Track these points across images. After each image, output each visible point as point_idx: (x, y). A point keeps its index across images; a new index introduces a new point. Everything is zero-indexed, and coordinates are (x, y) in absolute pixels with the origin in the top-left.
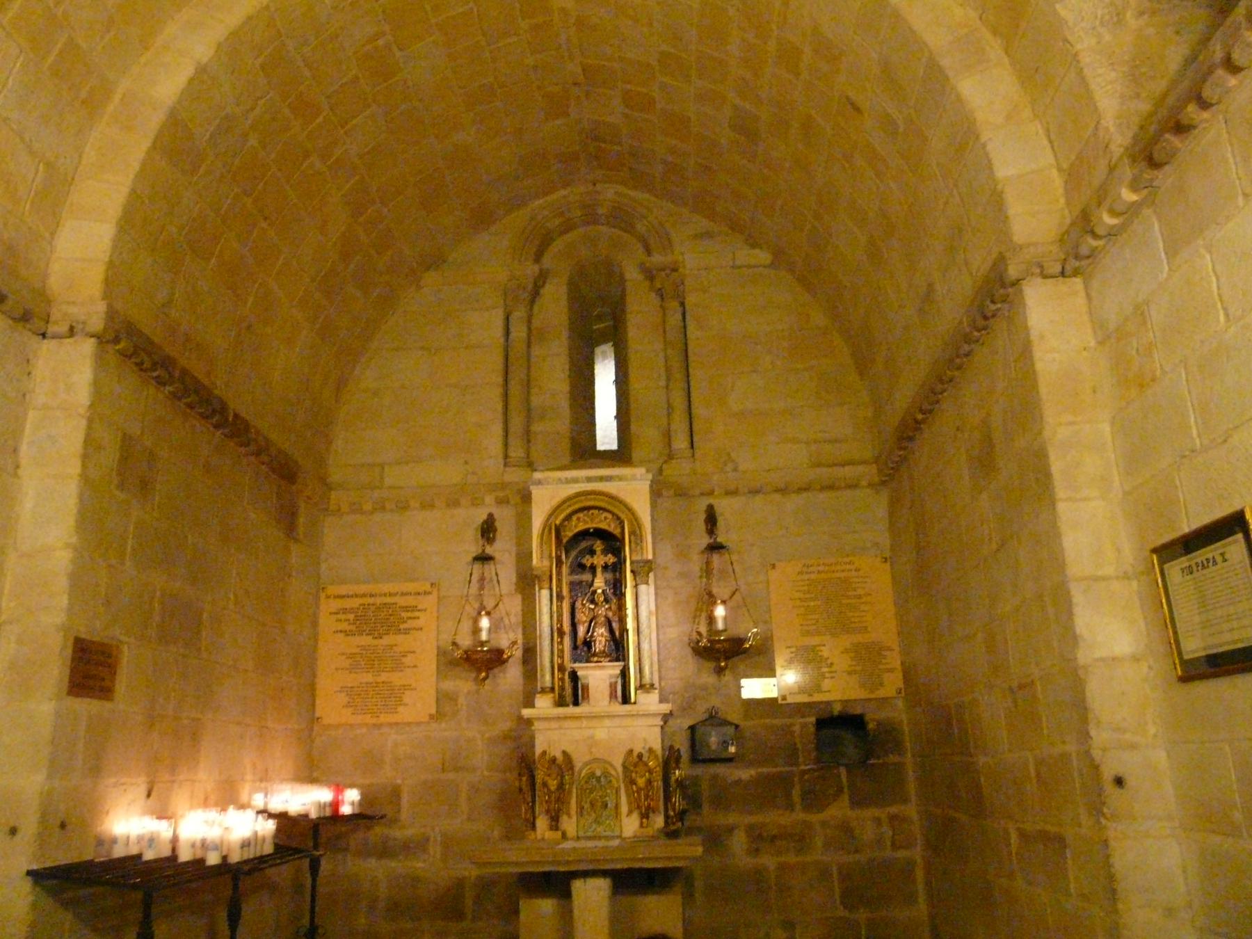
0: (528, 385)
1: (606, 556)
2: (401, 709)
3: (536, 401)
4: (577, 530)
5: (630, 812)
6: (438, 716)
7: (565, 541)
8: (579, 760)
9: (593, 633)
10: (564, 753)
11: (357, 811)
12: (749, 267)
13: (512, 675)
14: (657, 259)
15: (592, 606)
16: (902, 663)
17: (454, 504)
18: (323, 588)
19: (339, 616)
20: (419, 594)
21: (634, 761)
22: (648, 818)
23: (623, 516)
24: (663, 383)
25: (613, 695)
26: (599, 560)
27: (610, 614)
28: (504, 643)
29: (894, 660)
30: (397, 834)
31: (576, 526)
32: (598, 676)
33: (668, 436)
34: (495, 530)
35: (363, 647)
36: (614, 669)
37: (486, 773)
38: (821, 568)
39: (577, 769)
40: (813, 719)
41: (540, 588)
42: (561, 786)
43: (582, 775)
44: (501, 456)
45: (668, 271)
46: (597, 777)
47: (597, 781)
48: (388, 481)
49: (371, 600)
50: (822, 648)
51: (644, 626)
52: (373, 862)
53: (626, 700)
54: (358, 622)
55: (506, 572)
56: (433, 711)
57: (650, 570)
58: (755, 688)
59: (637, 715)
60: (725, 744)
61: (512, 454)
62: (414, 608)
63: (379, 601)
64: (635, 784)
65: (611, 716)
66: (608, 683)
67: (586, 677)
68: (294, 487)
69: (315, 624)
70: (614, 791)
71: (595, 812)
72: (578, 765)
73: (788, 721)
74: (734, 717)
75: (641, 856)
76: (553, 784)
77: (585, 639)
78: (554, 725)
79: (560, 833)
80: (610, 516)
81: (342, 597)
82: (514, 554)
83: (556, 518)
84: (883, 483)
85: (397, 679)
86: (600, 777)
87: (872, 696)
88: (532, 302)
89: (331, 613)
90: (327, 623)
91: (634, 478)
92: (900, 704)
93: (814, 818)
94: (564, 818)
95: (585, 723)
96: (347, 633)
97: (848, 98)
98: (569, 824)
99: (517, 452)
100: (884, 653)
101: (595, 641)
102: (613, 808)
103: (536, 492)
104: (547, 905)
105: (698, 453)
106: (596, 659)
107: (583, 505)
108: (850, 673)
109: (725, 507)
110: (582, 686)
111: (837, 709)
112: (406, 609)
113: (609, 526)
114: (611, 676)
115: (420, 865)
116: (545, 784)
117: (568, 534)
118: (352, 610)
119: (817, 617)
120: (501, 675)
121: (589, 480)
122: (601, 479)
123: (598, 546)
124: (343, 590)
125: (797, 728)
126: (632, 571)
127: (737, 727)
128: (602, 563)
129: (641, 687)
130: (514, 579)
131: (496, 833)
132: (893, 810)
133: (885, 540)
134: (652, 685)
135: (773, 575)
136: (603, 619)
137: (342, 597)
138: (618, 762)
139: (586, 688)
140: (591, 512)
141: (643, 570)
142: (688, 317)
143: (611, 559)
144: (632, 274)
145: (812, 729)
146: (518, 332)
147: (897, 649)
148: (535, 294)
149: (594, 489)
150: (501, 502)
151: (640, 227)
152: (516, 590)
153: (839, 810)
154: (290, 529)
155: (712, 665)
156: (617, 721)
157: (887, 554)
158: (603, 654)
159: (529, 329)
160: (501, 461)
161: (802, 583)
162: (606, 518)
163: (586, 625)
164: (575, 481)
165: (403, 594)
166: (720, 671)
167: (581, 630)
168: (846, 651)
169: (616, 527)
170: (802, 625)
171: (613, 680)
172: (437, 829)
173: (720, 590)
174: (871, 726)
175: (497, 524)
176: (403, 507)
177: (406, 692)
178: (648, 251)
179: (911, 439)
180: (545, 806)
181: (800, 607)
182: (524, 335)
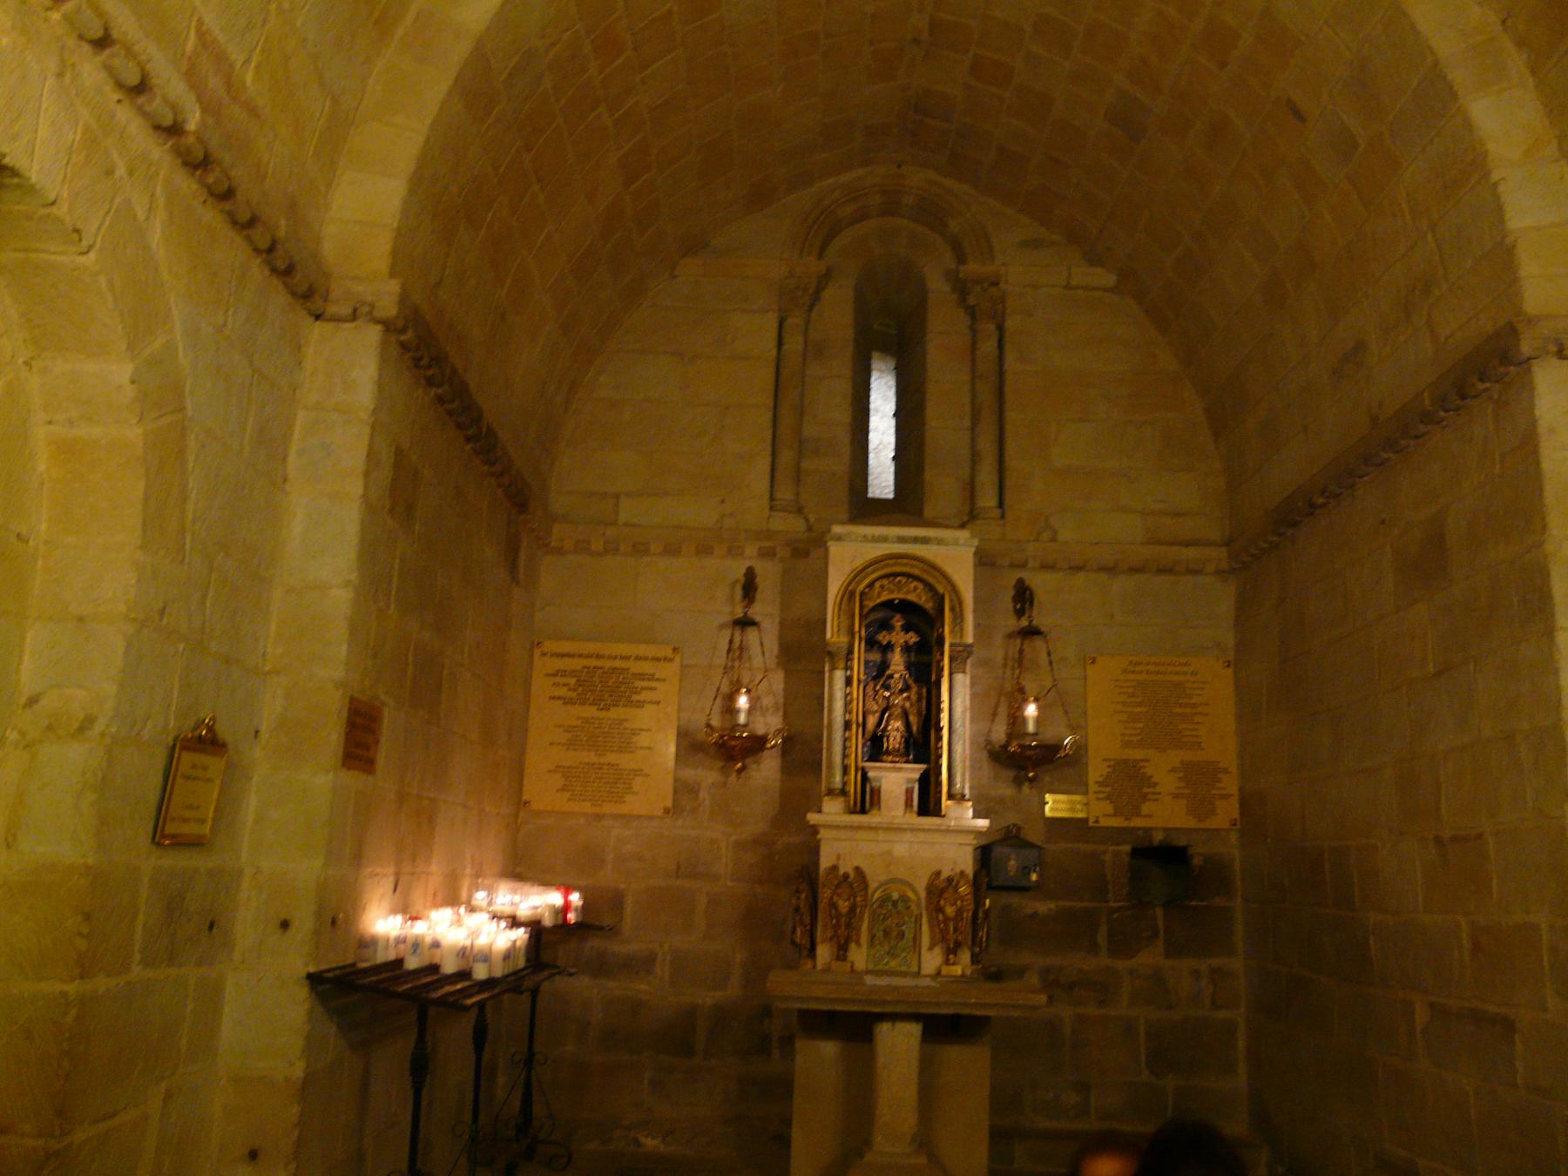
1: (907, 632)
2: (628, 798)
3: (809, 431)
4: (879, 601)
5: (930, 949)
6: (674, 811)
7: (866, 611)
9: (887, 726)
10: (858, 869)
11: (580, 919)
12: (1087, 288)
13: (767, 769)
14: (973, 268)
15: (887, 694)
16: (1241, 789)
17: (704, 550)
18: (538, 644)
19: (558, 679)
20: (658, 660)
21: (939, 889)
22: (955, 954)
23: (941, 590)
24: (967, 423)
25: (908, 803)
26: (899, 637)
27: (908, 704)
28: (760, 730)
29: (1231, 785)
30: (618, 948)
31: (879, 595)
33: (971, 490)
34: (756, 589)
35: (586, 721)
36: (914, 771)
37: (729, 884)
38: (1151, 668)
39: (870, 891)
40: (1127, 848)
41: (833, 669)
42: (853, 909)
43: (874, 900)
44: (767, 496)
45: (986, 285)
46: (893, 902)
47: (893, 907)
48: (622, 518)
49: (594, 663)
50: (1146, 764)
51: (959, 724)
52: (584, 981)
54: (581, 689)
55: (763, 644)
56: (669, 803)
57: (970, 654)
58: (1054, 805)
59: (948, 831)
60: (1026, 871)
61: (778, 495)
62: (651, 677)
63: (608, 664)
64: (943, 913)
65: (914, 830)
66: (904, 787)
67: (879, 780)
68: (522, 517)
69: (527, 683)
70: (913, 919)
71: (889, 943)
72: (873, 885)
73: (1101, 848)
74: (1034, 835)
75: (973, 1001)
76: (844, 906)
77: (875, 733)
78: (843, 834)
79: (849, 965)
80: (921, 586)
81: (562, 656)
82: (777, 620)
83: (859, 583)
84: (1233, 571)
85: (626, 761)
86: (897, 901)
87: (1202, 825)
88: (810, 309)
89: (547, 675)
90: (541, 686)
91: (956, 543)
92: (1233, 837)
93: (1121, 965)
94: (853, 946)
95: (882, 836)
96: (568, 702)
97: (1289, 101)
98: (859, 956)
99: (785, 494)
100: (1220, 775)
101: (888, 737)
102: (911, 939)
103: (834, 548)
104: (829, 1049)
105: (1009, 516)
106: (890, 758)
107: (894, 568)
108: (1176, 796)
109: (1040, 582)
110: (872, 790)
111: (1158, 837)
112: (641, 676)
113: (920, 598)
114: (909, 781)
115: (643, 987)
116: (834, 906)
118: (573, 673)
119: (1141, 725)
120: (754, 766)
121: (902, 540)
122: (916, 540)
123: (898, 622)
124: (565, 647)
125: (1108, 857)
126: (951, 659)
127: (1040, 848)
128: (902, 641)
129: (950, 796)
130: (776, 651)
131: (738, 956)
132: (1216, 962)
133: (1230, 640)
134: (964, 796)
135: (1091, 670)
136: (899, 710)
137: (562, 656)
138: (921, 885)
139: (876, 793)
140: (898, 578)
141: (961, 655)
142: (1008, 347)
143: (913, 638)
144: (937, 286)
145: (1126, 859)
146: (794, 344)
147: (1234, 769)
148: (816, 298)
149: (902, 551)
151: (954, 226)
152: (778, 664)
153: (1150, 958)
154: (513, 568)
155: (1011, 774)
156: (922, 837)
157: (1231, 657)
159: (806, 342)
160: (765, 502)
161: (1128, 684)
162: (915, 588)
163: (877, 715)
164: (884, 539)
165: (638, 658)
168: (1174, 770)
169: (927, 601)
170: (1123, 735)
171: (910, 785)
172: (666, 947)
173: (1030, 686)
174: (1196, 861)
175: (758, 580)
176: (640, 549)
177: (637, 778)
178: (961, 260)
179: (1295, 524)
180: (830, 933)
181: (1121, 712)
182: (800, 347)
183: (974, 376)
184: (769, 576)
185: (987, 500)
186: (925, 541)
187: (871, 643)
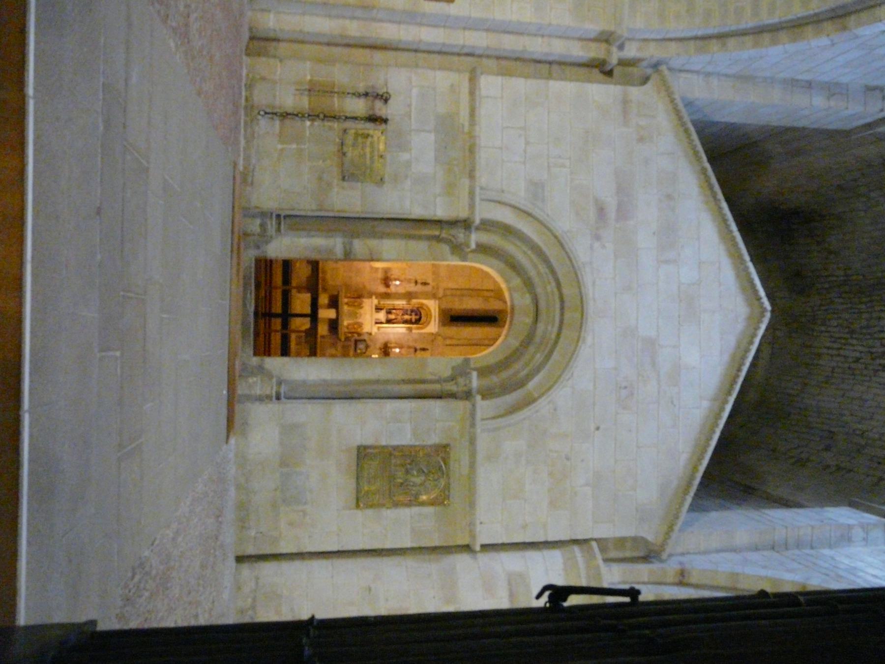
0: (471, 296)
3: (464, 298)
8: (362, 311)
13: (382, 289)
21: (360, 325)
25: (376, 319)
26: (414, 318)
28: (391, 287)
32: (382, 316)
33: (451, 338)
53: (377, 323)
60: (360, 349)
65: (372, 320)
107: (429, 315)
116: (356, 302)
117: (421, 310)
121: (435, 317)
123: (417, 317)
138: (360, 320)
141: (410, 329)
143: (413, 320)
150: (433, 287)
158: (387, 317)
164: (435, 313)
166: (381, 349)
167: (394, 311)
173: (404, 351)
175: (427, 286)
183: (481, 339)
184: (427, 289)
185: (448, 342)
186: (435, 321)
187: (412, 311)
